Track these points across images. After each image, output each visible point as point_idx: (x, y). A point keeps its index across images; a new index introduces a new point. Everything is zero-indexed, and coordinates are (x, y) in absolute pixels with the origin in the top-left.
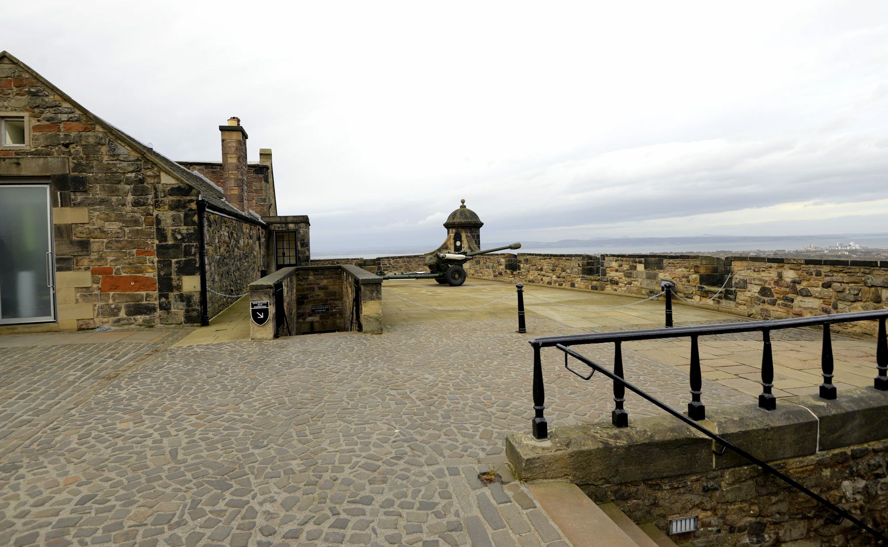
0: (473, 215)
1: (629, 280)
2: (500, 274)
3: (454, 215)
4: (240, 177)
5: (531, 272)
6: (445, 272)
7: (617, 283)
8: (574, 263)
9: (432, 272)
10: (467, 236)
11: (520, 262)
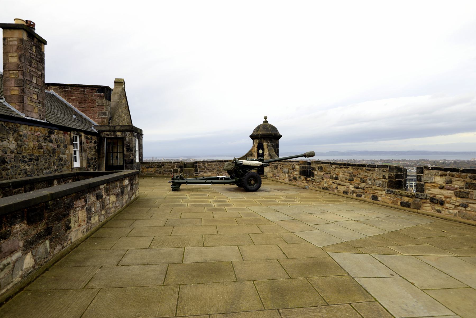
0: (274, 128)
1: (464, 201)
2: (295, 179)
3: (258, 128)
4: (21, 77)
5: (325, 180)
6: (243, 177)
7: (442, 203)
8: (377, 174)
9: (232, 178)
10: (268, 146)
11: (314, 169)
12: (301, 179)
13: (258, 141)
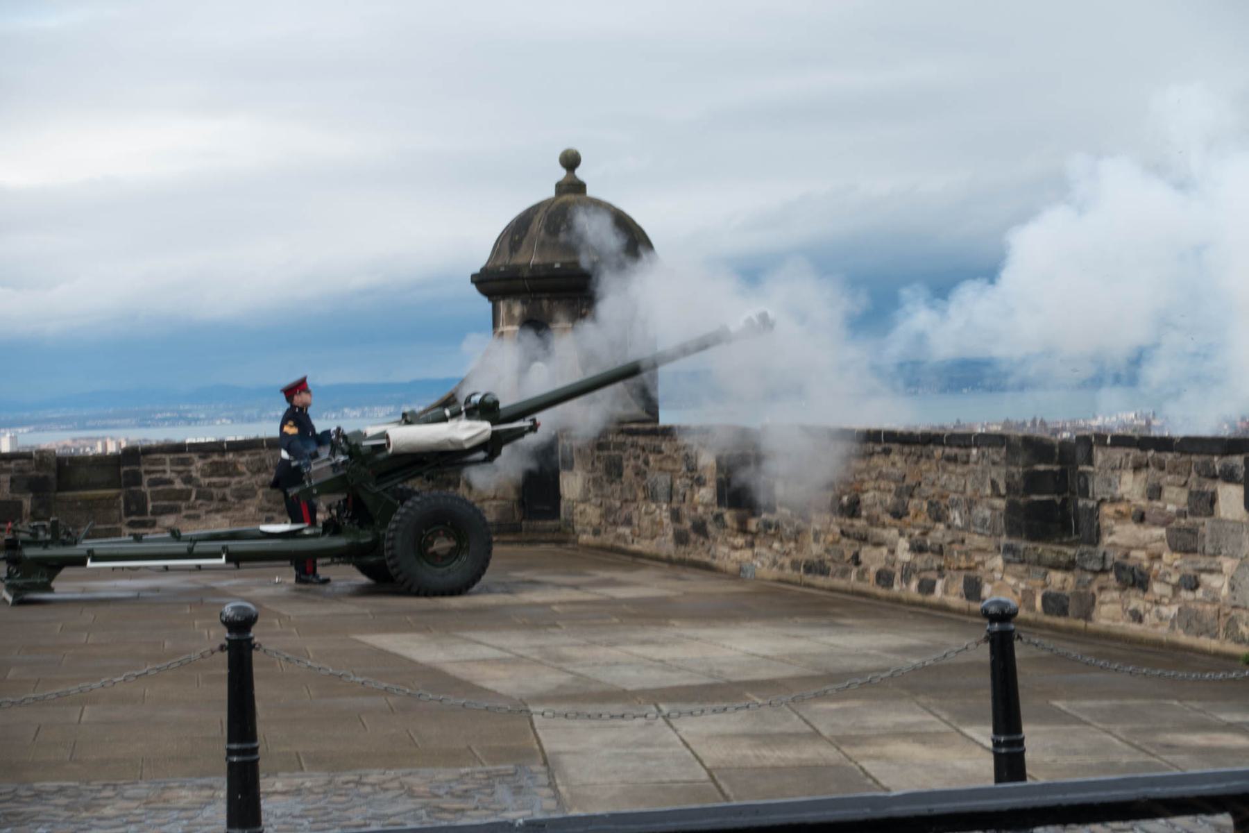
12: (724, 526)
13: (518, 309)
